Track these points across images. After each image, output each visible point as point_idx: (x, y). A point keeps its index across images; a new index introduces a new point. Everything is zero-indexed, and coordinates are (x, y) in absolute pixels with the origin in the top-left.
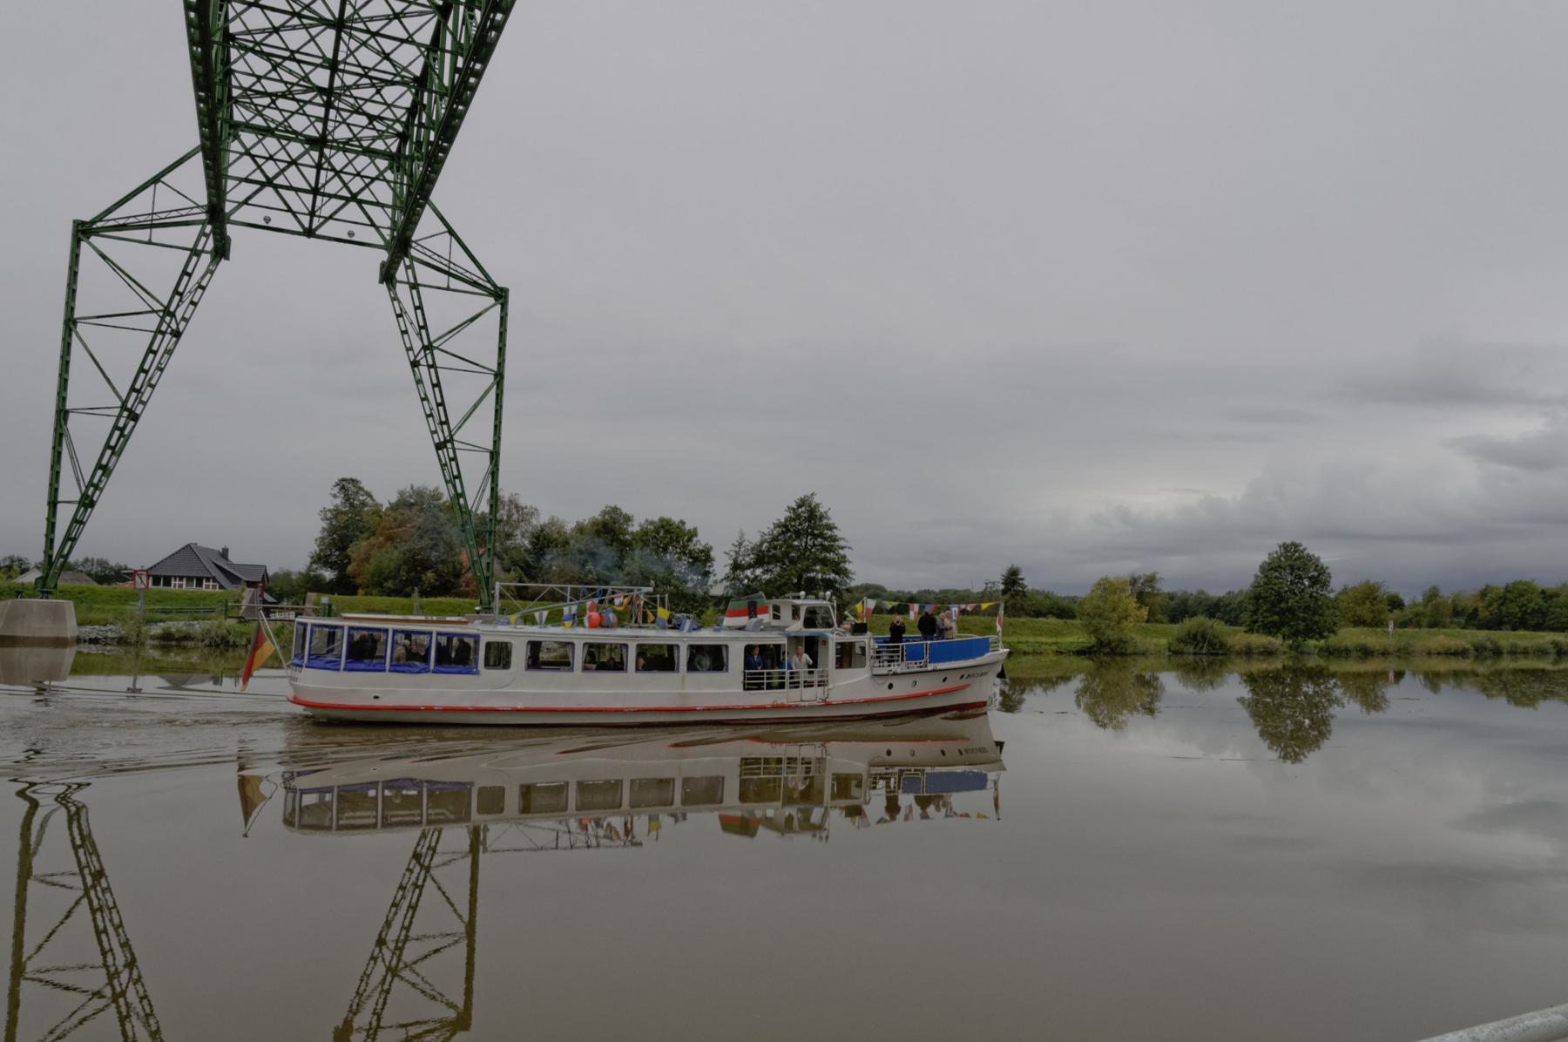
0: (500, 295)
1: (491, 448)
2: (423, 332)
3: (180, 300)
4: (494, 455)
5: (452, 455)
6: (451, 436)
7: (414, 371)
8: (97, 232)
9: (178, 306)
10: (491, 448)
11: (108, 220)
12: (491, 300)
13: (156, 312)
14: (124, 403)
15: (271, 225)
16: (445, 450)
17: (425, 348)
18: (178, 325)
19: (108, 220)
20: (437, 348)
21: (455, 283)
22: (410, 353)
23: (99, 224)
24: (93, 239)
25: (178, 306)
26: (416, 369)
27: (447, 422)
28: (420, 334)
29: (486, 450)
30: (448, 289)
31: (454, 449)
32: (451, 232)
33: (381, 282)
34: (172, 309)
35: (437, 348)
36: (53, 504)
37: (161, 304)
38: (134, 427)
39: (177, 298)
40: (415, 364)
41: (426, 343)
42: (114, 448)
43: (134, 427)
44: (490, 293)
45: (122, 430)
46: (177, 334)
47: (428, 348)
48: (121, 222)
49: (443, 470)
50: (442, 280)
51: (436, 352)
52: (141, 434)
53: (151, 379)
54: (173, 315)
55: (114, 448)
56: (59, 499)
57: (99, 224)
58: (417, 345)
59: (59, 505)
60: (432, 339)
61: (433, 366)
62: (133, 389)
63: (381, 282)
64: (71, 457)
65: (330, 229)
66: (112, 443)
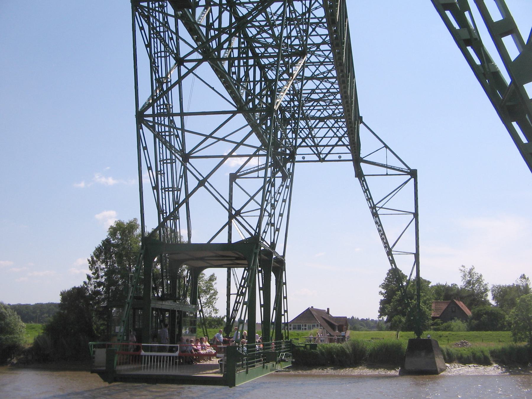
0: (413, 174)
1: (415, 252)
4: (417, 255)
8: (238, 177)
10: (415, 252)
11: (241, 172)
12: (409, 177)
15: (305, 160)
19: (241, 172)
21: (390, 171)
23: (238, 174)
24: (237, 180)
29: (413, 254)
30: (387, 175)
32: (386, 146)
33: (356, 177)
36: (229, 295)
44: (408, 174)
48: (245, 172)
50: (383, 171)
56: (231, 293)
57: (238, 174)
59: (231, 296)
63: (356, 177)
64: (234, 275)
65: (329, 158)
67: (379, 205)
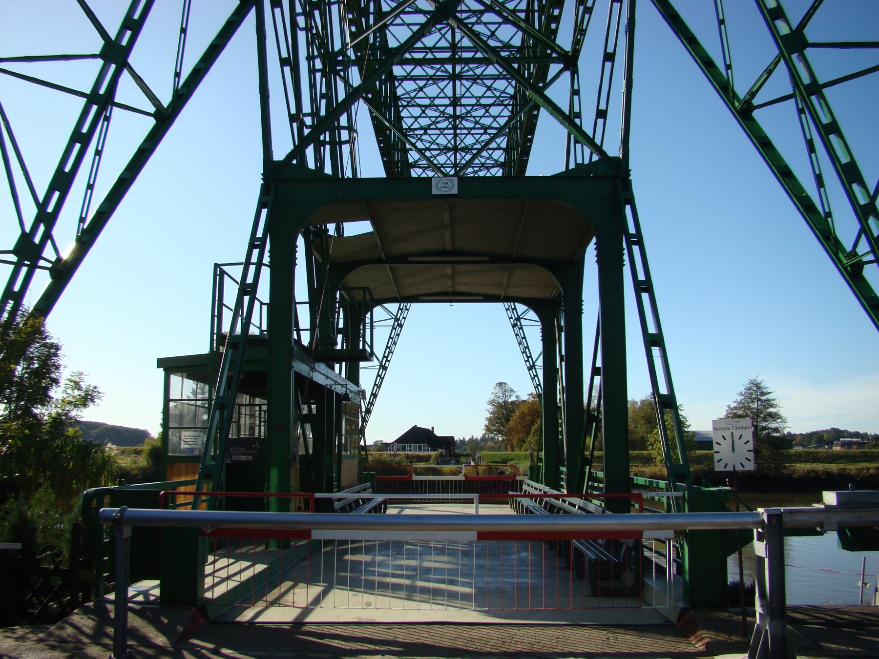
2: (514, 311)
3: (402, 312)
5: (535, 374)
6: (534, 363)
7: (514, 330)
9: (401, 314)
13: (393, 318)
14: (381, 363)
16: (534, 370)
17: (516, 319)
18: (401, 322)
20: (522, 318)
22: (511, 320)
25: (401, 314)
26: (515, 328)
27: (531, 357)
28: (513, 312)
31: (535, 369)
34: (398, 317)
35: (522, 318)
37: (394, 315)
38: (385, 374)
39: (400, 311)
40: (514, 326)
41: (516, 317)
42: (378, 386)
43: (385, 374)
45: (380, 376)
46: (401, 326)
47: (518, 319)
49: (533, 381)
51: (521, 320)
52: (389, 375)
53: (391, 349)
54: (399, 319)
55: (378, 386)
58: (514, 319)
60: (519, 315)
61: (521, 328)
62: (384, 357)
66: (377, 383)
67: (521, 317)
